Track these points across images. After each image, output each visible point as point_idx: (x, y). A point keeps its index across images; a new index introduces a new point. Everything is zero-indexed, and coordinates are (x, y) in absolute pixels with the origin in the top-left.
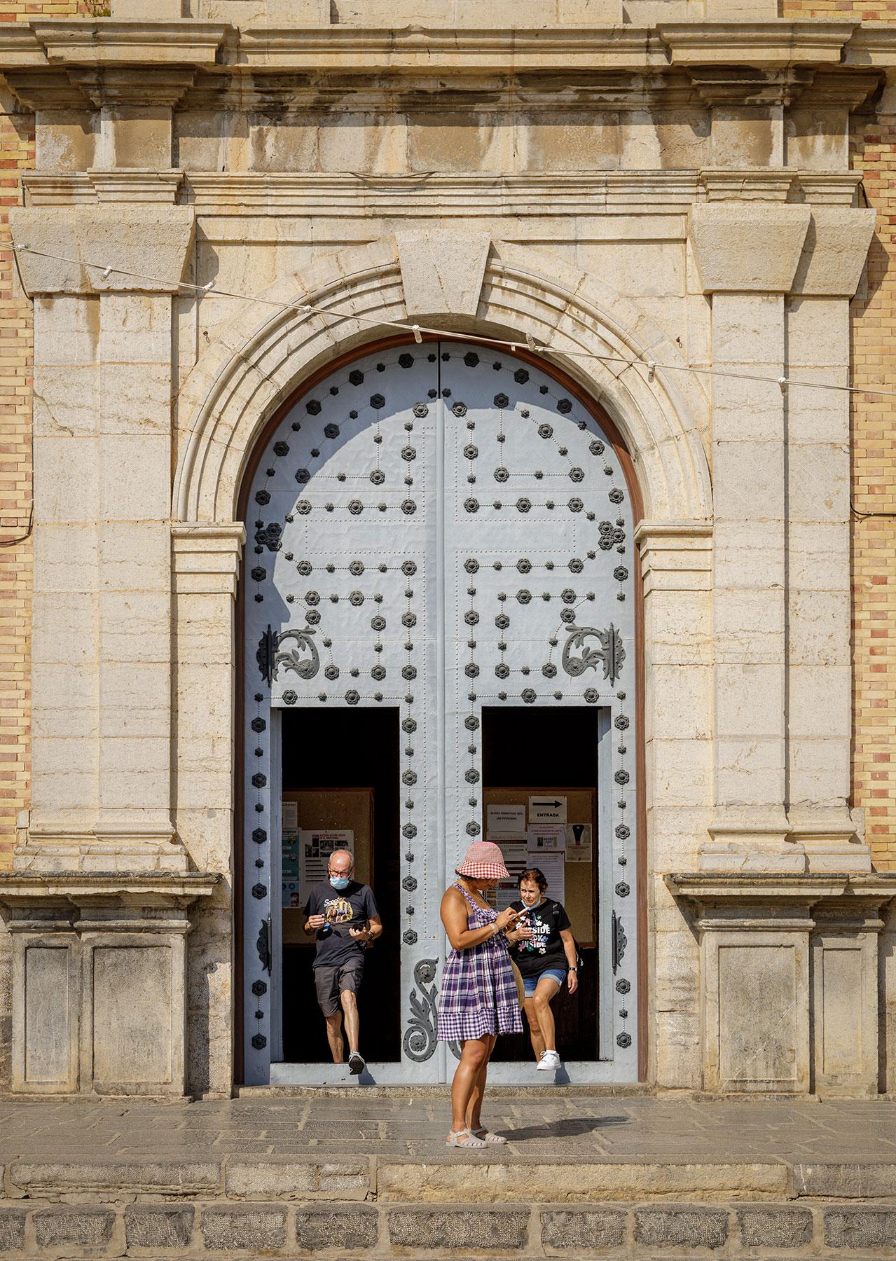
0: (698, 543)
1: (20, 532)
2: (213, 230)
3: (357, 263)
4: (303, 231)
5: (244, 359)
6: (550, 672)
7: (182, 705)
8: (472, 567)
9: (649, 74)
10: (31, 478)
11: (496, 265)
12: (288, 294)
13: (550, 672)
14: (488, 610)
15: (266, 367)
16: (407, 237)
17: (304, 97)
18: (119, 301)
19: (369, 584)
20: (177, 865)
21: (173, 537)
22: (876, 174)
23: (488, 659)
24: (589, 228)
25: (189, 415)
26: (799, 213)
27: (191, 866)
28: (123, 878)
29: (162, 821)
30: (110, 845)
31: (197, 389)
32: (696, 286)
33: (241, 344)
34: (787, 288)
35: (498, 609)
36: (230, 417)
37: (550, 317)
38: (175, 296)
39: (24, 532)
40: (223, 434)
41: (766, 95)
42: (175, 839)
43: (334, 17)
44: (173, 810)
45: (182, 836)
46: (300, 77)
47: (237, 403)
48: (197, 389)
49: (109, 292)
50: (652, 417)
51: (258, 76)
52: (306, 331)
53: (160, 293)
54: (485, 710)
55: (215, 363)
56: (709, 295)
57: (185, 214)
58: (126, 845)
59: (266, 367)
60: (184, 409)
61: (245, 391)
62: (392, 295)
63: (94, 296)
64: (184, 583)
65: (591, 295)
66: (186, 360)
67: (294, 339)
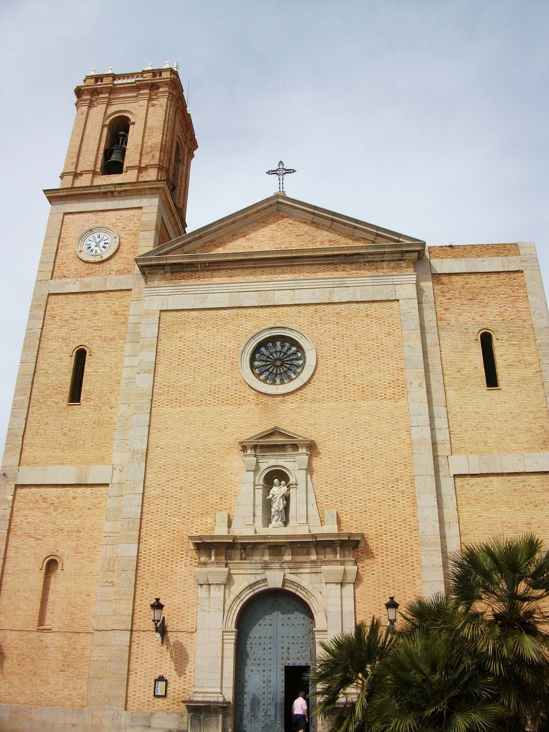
0: (325, 633)
1: (194, 630)
2: (232, 572)
3: (259, 578)
4: (249, 572)
5: (237, 596)
6: (298, 659)
7: (224, 666)
8: (283, 637)
9: (313, 541)
10: (197, 619)
11: (285, 578)
12: (246, 584)
13: (298, 659)
14: (286, 646)
15: (242, 598)
16: (268, 573)
17: (250, 546)
18: (214, 586)
19: (262, 641)
20: (221, 700)
21: (223, 632)
22: (358, 558)
23: (285, 655)
24: (302, 571)
25: (227, 607)
26: (342, 567)
27: (224, 699)
28: (209, 702)
29: (219, 690)
30: (208, 695)
31: (229, 602)
32: (323, 581)
33: (237, 594)
34: (341, 582)
35: (288, 646)
36: (235, 608)
37: (296, 588)
38: (225, 585)
39: (194, 630)
40: (233, 611)
41: (336, 545)
42: (221, 693)
43: (256, 532)
44: (221, 688)
45: (223, 693)
46: (249, 543)
47: (236, 605)
48: (229, 602)
49: (213, 584)
50: (315, 607)
51: (241, 543)
52: (250, 591)
53: (221, 584)
54: (285, 667)
55: (232, 597)
56: (326, 583)
57: (227, 569)
58: (211, 695)
59: (242, 598)
60: (226, 606)
61: (237, 603)
62: (266, 584)
63: (210, 585)
64: (225, 641)
65: (303, 584)
66: (227, 596)
67: (247, 593)
